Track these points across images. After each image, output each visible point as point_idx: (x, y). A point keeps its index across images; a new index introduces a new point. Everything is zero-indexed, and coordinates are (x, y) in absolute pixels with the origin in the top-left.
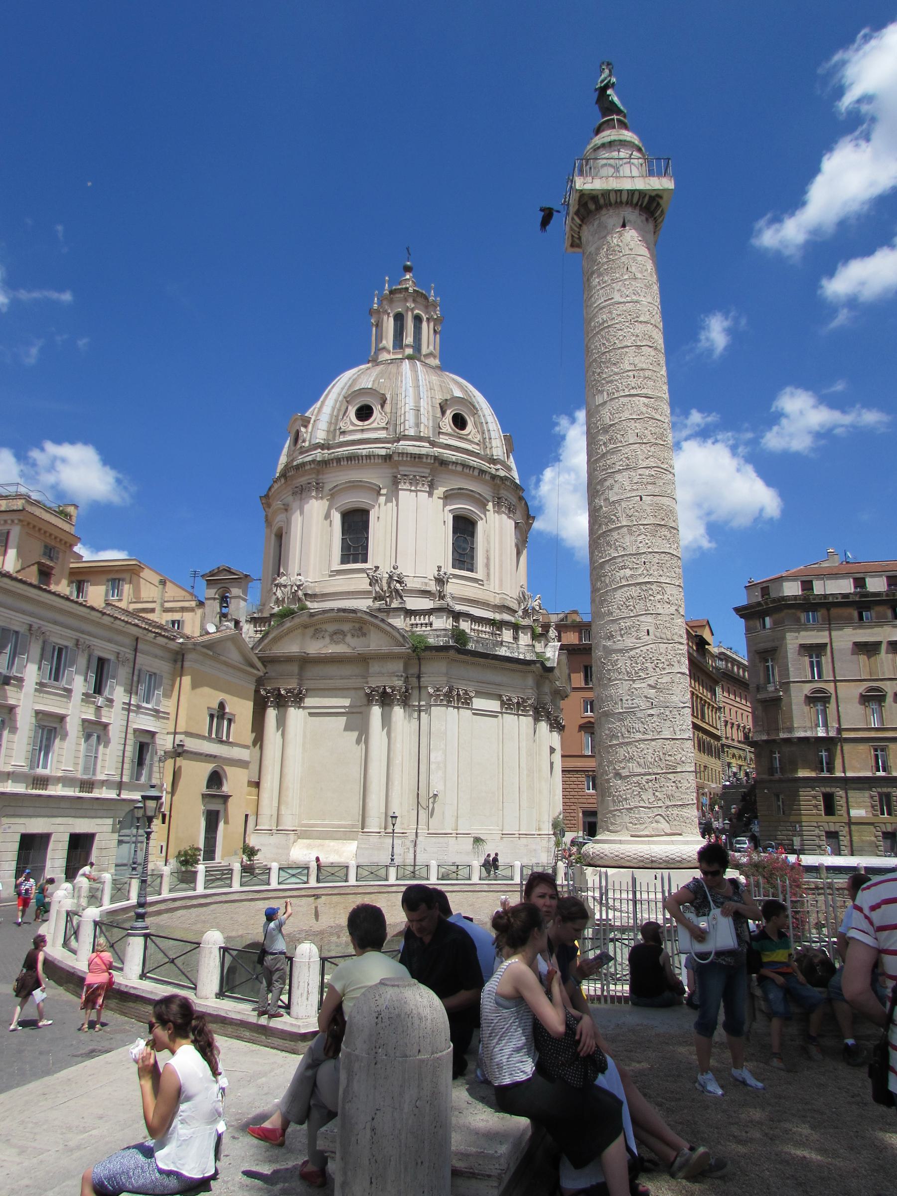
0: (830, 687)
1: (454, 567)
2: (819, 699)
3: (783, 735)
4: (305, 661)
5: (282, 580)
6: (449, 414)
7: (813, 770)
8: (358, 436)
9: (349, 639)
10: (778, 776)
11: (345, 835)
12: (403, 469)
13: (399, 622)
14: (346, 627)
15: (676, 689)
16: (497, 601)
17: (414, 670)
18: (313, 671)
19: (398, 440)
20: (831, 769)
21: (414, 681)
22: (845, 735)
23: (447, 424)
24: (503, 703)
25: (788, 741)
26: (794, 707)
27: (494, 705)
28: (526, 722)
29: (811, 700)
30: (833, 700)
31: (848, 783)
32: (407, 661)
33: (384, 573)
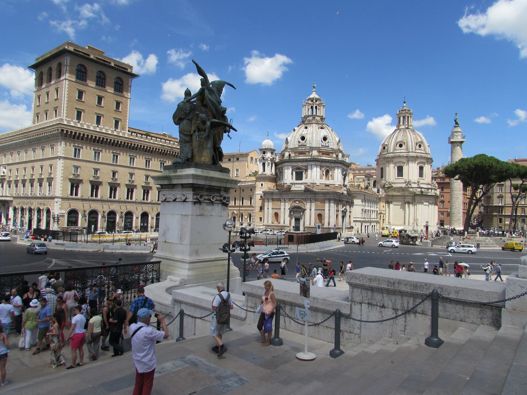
0: (504, 194)
1: (419, 177)
2: (500, 197)
3: (491, 205)
4: (393, 196)
5: (388, 181)
6: (418, 145)
7: (498, 213)
8: (399, 151)
9: (401, 192)
10: (489, 214)
11: (401, 225)
12: (410, 159)
13: (411, 190)
14: (400, 190)
15: (461, 210)
16: (427, 183)
17: (414, 198)
18: (394, 198)
19: (408, 153)
20: (502, 213)
21: (414, 200)
22: (506, 205)
23: (417, 147)
24: (429, 203)
25: (492, 206)
26: (494, 198)
27: (427, 204)
28: (433, 206)
29: (498, 197)
30: (504, 197)
31: (505, 216)
32: (412, 196)
33: (407, 180)
